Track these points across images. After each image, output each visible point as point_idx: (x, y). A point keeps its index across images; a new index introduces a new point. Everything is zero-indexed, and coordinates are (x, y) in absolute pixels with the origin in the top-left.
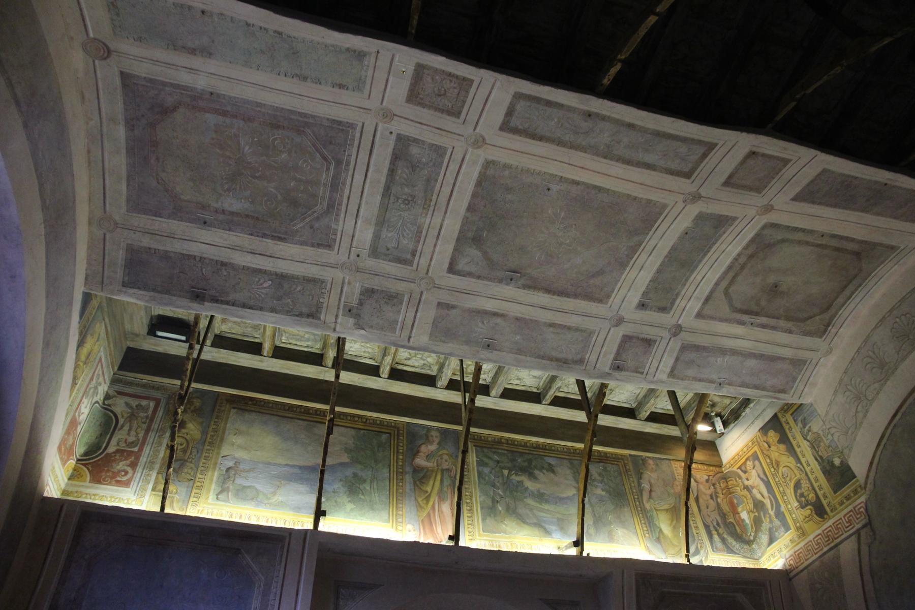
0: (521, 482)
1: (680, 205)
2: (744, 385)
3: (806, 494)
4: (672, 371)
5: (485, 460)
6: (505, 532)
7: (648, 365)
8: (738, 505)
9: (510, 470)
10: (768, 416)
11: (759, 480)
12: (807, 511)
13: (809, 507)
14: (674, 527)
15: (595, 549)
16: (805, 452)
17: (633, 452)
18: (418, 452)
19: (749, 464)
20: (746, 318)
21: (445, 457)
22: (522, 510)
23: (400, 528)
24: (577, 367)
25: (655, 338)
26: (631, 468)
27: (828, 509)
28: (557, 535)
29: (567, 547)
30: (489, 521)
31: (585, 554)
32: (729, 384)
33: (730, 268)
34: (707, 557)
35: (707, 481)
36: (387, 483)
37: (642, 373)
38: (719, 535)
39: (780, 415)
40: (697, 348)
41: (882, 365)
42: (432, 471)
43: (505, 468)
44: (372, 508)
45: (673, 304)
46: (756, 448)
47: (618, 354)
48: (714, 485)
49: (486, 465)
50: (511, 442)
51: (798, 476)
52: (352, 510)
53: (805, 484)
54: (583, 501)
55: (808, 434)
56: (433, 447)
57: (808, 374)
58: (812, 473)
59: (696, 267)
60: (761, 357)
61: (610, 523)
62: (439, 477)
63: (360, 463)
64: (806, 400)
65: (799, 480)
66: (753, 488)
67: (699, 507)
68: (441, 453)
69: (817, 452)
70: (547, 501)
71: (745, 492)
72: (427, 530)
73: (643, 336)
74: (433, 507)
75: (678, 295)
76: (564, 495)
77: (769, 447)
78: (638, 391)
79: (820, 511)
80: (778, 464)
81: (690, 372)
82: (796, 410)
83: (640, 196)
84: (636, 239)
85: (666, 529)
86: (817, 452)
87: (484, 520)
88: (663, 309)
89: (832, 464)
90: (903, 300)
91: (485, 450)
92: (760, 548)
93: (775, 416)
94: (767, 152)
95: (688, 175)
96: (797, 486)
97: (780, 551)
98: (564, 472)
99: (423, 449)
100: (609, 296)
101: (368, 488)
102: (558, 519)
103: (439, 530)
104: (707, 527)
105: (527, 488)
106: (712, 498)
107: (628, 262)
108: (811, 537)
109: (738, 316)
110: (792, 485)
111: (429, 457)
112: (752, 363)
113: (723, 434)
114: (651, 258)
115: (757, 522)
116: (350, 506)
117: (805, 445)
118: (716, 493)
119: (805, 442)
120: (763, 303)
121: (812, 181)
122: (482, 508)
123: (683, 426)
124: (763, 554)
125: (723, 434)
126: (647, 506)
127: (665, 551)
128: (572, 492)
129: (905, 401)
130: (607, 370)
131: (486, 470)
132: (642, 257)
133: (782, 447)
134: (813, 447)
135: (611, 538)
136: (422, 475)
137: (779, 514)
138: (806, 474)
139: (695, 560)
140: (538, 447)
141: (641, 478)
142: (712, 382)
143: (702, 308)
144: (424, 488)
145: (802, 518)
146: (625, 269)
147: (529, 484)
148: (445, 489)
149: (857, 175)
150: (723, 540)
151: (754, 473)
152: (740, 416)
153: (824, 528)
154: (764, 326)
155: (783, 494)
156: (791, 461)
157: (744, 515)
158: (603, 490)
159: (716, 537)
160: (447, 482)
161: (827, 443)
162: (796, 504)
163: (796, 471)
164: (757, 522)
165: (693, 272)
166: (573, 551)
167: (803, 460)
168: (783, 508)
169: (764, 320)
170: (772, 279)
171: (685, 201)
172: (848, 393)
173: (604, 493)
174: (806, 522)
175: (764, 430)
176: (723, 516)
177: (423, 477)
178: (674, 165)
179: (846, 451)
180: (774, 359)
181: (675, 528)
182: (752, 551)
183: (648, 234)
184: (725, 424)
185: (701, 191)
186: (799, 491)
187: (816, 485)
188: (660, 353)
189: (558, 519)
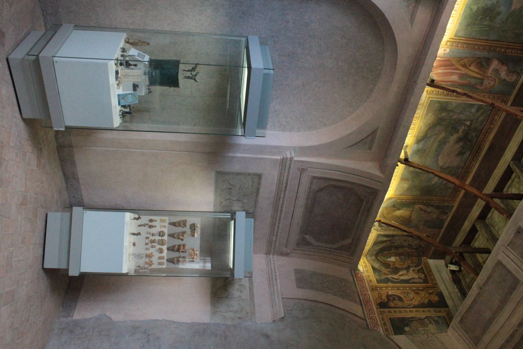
0: (458, 132)
2: (475, 302)
3: (394, 302)
4: (502, 264)
5: (482, 111)
6: (426, 114)
7: (513, 252)
9: (468, 127)
10: (449, 302)
11: (411, 277)
12: (384, 297)
13: (386, 300)
14: (398, 218)
15: (400, 169)
17: (454, 209)
18: (503, 64)
19: (423, 276)
21: (492, 83)
22: (438, 128)
23: (449, 44)
26: (445, 204)
28: (415, 147)
29: (406, 153)
30: (437, 105)
31: (399, 163)
32: (478, 294)
34: (375, 230)
35: (420, 246)
36: (484, 38)
37: (508, 245)
38: (386, 241)
39: (447, 309)
42: (485, 72)
43: (470, 124)
44: (468, 25)
46: (430, 284)
48: (417, 249)
49: (477, 111)
50: (489, 131)
51: (406, 302)
52: (471, 9)
53: (400, 304)
54: (433, 173)
56: (503, 75)
58: (405, 311)
61: (413, 181)
62: (478, 76)
63: (507, 19)
66: (408, 271)
67: (406, 236)
68: (497, 80)
69: (416, 320)
70: (439, 146)
72: (442, 63)
74: (458, 69)
76: (440, 158)
77: (429, 293)
78: (496, 228)
79: (382, 305)
80: (417, 293)
82: (446, 321)
85: (398, 213)
86: (416, 320)
87: (439, 102)
89: (407, 325)
91: (489, 112)
92: (372, 260)
93: (446, 306)
96: (400, 299)
97: (367, 271)
98: (456, 162)
99: (504, 68)
101: (485, 23)
102: (425, 150)
103: (439, 71)
104: (393, 236)
105: (452, 135)
106: (409, 245)
108: (369, 293)
110: (402, 296)
111: (496, 71)
113: (447, 267)
116: (475, 8)
117: (422, 315)
118: (412, 248)
119: (425, 316)
122: (447, 102)
123: (461, 250)
124: (368, 261)
125: (447, 267)
126: (416, 206)
127: (386, 208)
128: (441, 163)
130: (520, 224)
131: (473, 110)
133: (426, 301)
134: (420, 319)
135: (403, 179)
136: (484, 64)
137: (387, 280)
138: (405, 308)
139: (376, 224)
140: (480, 148)
141: (436, 208)
144: (473, 64)
145: (382, 293)
147: (455, 136)
148: (468, 79)
150: (382, 242)
151: (416, 276)
152: (455, 284)
153: (372, 302)
155: (398, 288)
156: (416, 302)
157: (393, 259)
158: (436, 183)
159: (385, 239)
160: (473, 81)
162: (390, 293)
163: (408, 302)
164: (387, 265)
166: (402, 156)
167: (414, 310)
168: (390, 284)
173: (433, 182)
175: (440, 295)
176: (396, 247)
177: (482, 65)
179: (411, 337)
181: (398, 218)
182: (371, 255)
184: (452, 272)
189: (425, 150)
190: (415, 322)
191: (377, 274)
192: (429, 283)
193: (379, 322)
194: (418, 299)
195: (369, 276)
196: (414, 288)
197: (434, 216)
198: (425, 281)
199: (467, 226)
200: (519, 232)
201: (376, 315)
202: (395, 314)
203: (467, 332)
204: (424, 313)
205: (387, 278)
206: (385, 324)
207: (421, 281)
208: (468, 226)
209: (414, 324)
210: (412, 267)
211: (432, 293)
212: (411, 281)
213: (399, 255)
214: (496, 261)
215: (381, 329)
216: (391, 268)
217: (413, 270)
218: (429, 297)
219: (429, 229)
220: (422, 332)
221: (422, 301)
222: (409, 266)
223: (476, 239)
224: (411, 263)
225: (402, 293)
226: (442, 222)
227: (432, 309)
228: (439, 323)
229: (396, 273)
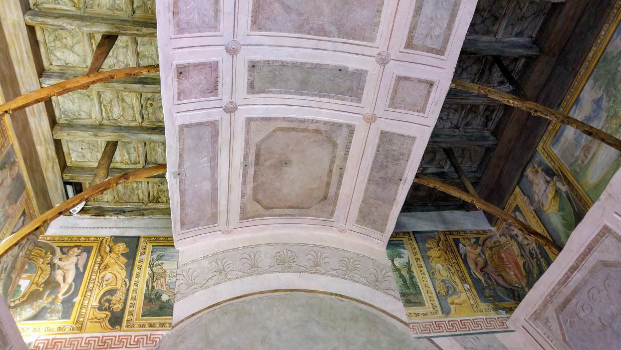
1: (375, 52)
4: (187, 126)
7: (189, 101)
8: (26, 271)
12: (102, 315)
16: (141, 276)
20: (252, 158)
24: (172, 29)
25: (220, 91)
27: (124, 323)
33: (303, 121)
37: (179, 99)
39: (142, 240)
40: (215, 135)
41: (253, 266)
45: (259, 92)
46: (95, 246)
47: (196, 65)
51: (119, 286)
53: (120, 295)
55: (156, 266)
57: (204, 231)
58: (135, 291)
59: (301, 94)
60: (214, 189)
64: (179, 246)
65: (117, 290)
66: (59, 268)
69: (153, 282)
71: (48, 268)
73: (220, 80)
75: (270, 92)
77: (110, 252)
78: (83, 116)
79: (116, 320)
81: (189, 143)
83: (383, 15)
84: (333, 29)
86: (153, 282)
88: (251, 87)
89: (158, 297)
90: (295, 244)
93: (139, 237)
94: (432, 94)
95: (409, 45)
96: (112, 292)
100: (260, 29)
107: (304, 32)
108: (85, 335)
109: (253, 151)
110: (106, 289)
112: (207, 186)
114: (311, 51)
115: (33, 296)
120: (268, 163)
121: (403, 136)
129: (252, 294)
130: (175, 62)
132: (309, 42)
133: (124, 260)
137: (68, 303)
138: (128, 290)
142: (180, 166)
143: (256, 119)
146: (295, 32)
149: (410, 160)
152: (104, 215)
154: (245, 175)
156: (123, 273)
161: (168, 281)
162: (96, 304)
163: (119, 283)
164: (33, 296)
165: (295, 93)
167: (134, 279)
168: (77, 300)
169: (251, 171)
170: (294, 157)
171: (379, 54)
172: (214, 264)
174: (91, 322)
175: (117, 239)
178: (420, 31)
179: (179, 296)
180: (214, 200)
183: (339, 37)
184: (83, 211)
185: (391, 62)
186: (108, 297)
187: (129, 301)
188: (205, 105)
190: (155, 284)
191: (48, 315)
192: (93, 247)
193: (148, 333)
194: (117, 267)
195: (48, 330)
196: (96, 268)
197: (9, 181)
198: (88, 250)
199: (45, 151)
200: (181, 73)
201: (133, 334)
202: (137, 306)
203: (197, 225)
204: (143, 268)
205: (63, 302)
206: (150, 325)
207: (85, 255)
208: (47, 150)
209: (158, 286)
210: (52, 259)
211: (111, 249)
212: (81, 270)
213: (22, 270)
214: (178, 129)
215: (159, 333)
216: (44, 290)
217: (60, 260)
218: (117, 254)
219: (18, 203)
220: (174, 279)
221: (124, 266)
222: (48, 264)
223: (70, 154)
224: (43, 258)
225: (101, 285)
226: (18, 178)
227: (138, 258)
228: (162, 256)
229: (57, 285)
